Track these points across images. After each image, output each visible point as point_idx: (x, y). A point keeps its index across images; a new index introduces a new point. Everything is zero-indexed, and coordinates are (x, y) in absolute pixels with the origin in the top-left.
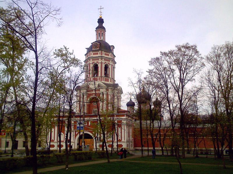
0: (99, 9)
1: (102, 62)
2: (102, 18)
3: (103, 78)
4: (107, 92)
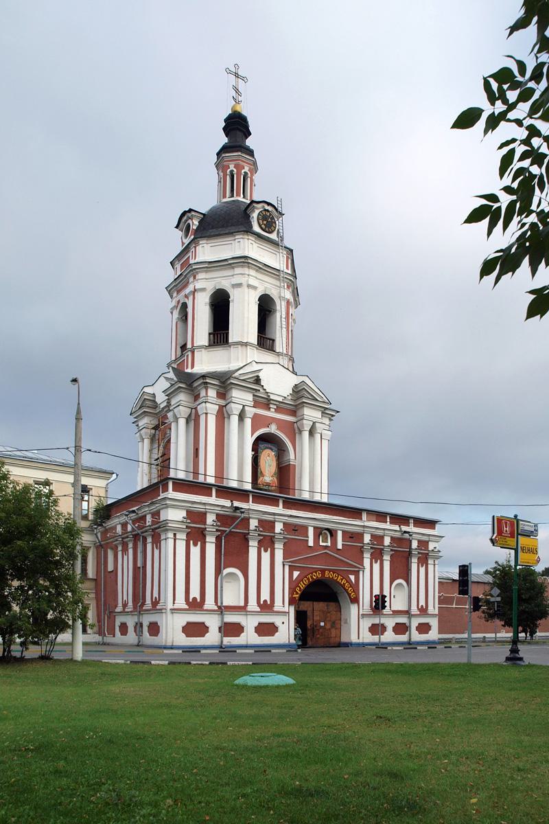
0: (229, 71)
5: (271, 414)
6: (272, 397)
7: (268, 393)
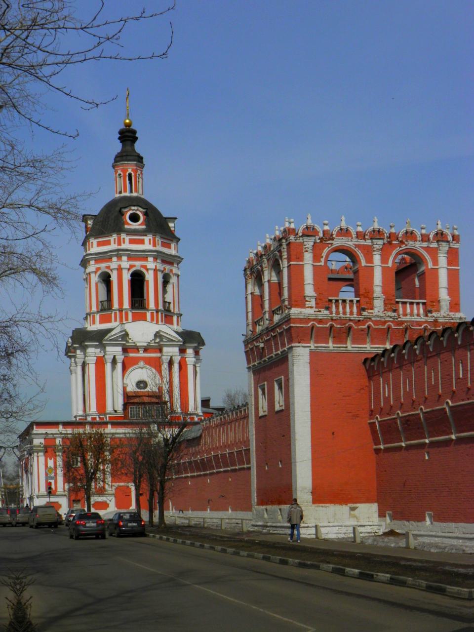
1: (156, 266)
2: (132, 127)
3: (162, 314)
4: (183, 355)
5: (141, 354)
6: (138, 344)
7: (134, 342)
